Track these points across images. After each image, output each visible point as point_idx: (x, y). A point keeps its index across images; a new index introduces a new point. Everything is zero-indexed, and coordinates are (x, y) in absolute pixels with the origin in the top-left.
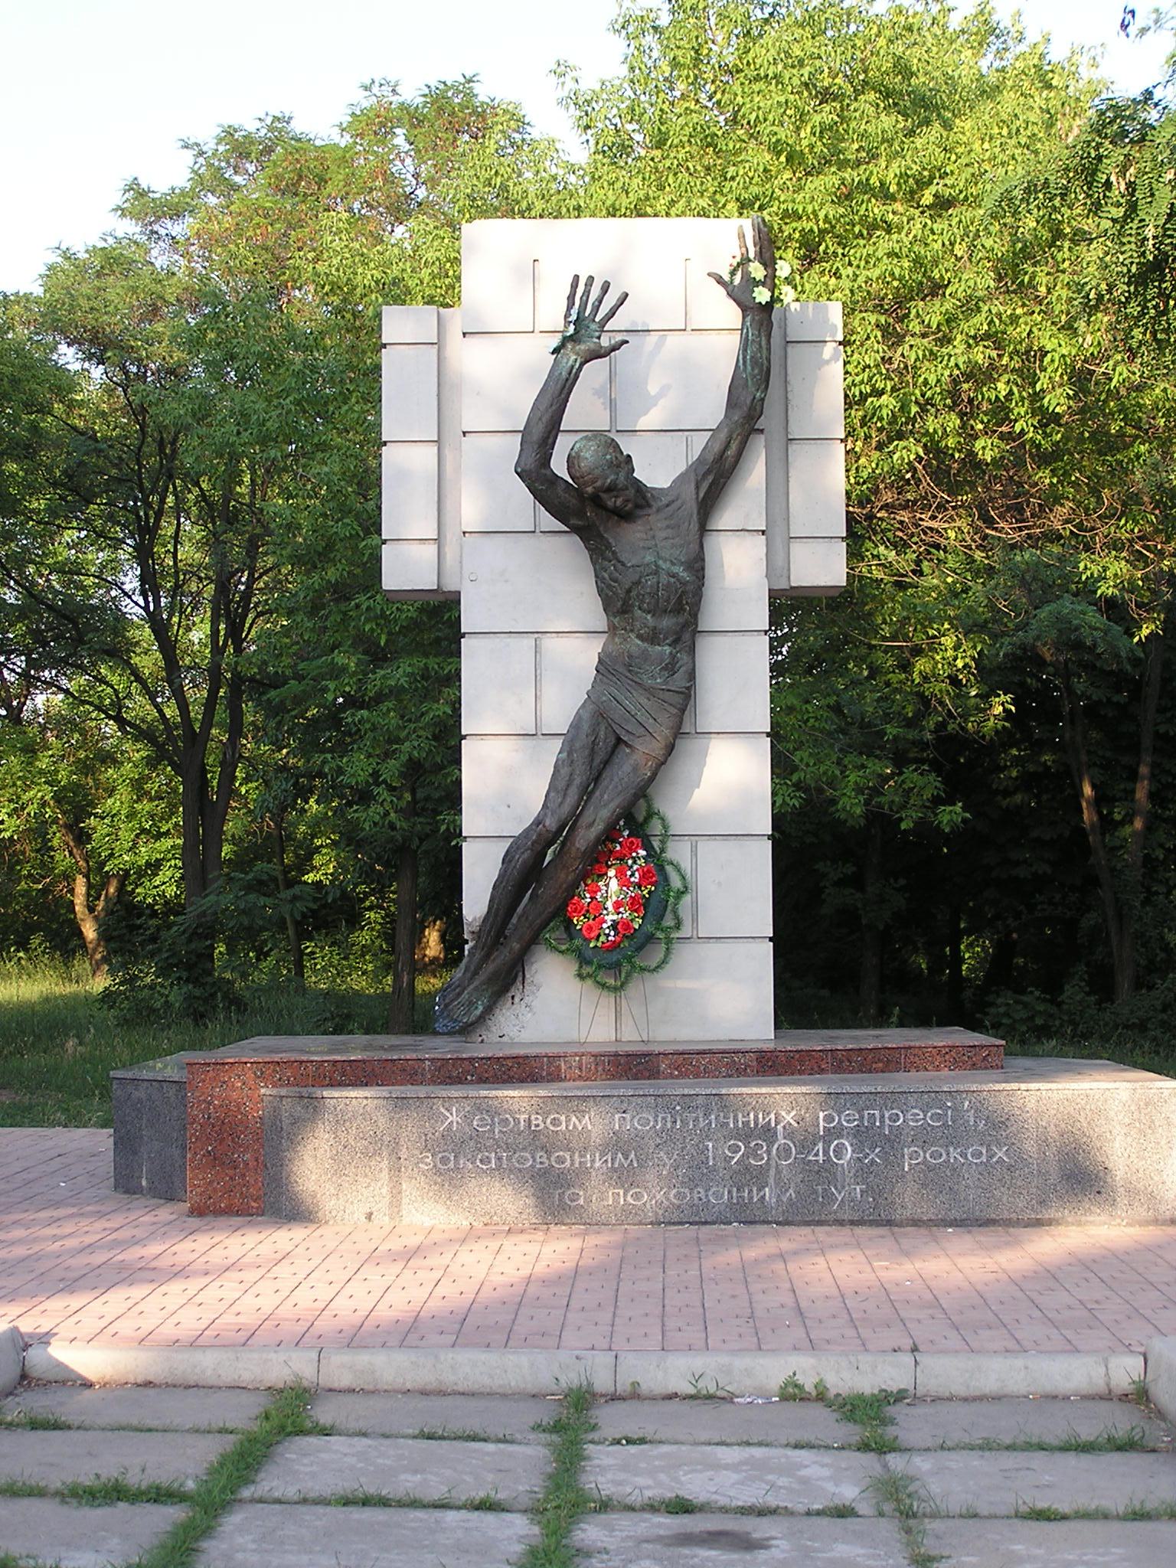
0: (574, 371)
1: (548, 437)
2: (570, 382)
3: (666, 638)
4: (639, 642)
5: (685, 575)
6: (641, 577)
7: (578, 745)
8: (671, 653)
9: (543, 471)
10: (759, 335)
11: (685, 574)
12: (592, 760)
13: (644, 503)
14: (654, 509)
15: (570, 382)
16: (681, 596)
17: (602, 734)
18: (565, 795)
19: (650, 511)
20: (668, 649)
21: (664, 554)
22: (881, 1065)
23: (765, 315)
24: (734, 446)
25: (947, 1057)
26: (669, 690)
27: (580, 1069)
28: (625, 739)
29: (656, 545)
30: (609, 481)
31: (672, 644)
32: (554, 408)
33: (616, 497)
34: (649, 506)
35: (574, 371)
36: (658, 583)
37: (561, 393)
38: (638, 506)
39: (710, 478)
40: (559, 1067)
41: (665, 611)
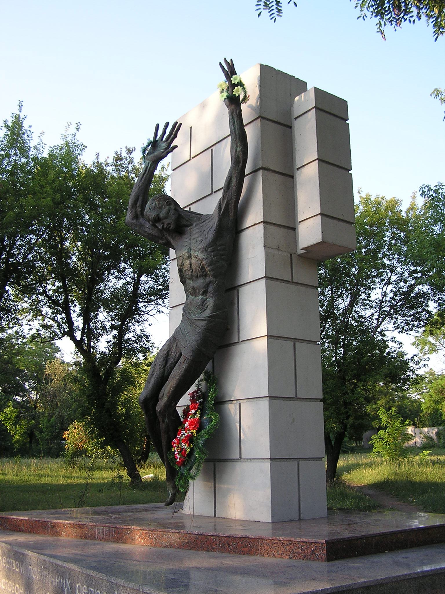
0: (148, 168)
1: (136, 204)
2: (146, 174)
3: (199, 292)
4: (191, 297)
5: (201, 256)
6: (182, 262)
7: (161, 354)
8: (201, 299)
9: (134, 221)
10: (233, 118)
11: (202, 255)
12: (166, 363)
13: (189, 223)
14: (194, 225)
15: (146, 174)
16: (203, 268)
17: (174, 348)
18: (149, 383)
19: (192, 227)
20: (201, 297)
21: (192, 248)
22: (246, 549)
23: (233, 107)
24: (234, 181)
25: (288, 548)
26: (198, 320)
27: (103, 534)
28: (181, 349)
29: (190, 244)
30: (153, 216)
31: (203, 294)
32: (137, 188)
33: (163, 223)
34: (192, 225)
35: (148, 168)
36: (191, 263)
37: (141, 181)
38: (188, 226)
39: (225, 201)
40: (95, 531)
41: (197, 277)
